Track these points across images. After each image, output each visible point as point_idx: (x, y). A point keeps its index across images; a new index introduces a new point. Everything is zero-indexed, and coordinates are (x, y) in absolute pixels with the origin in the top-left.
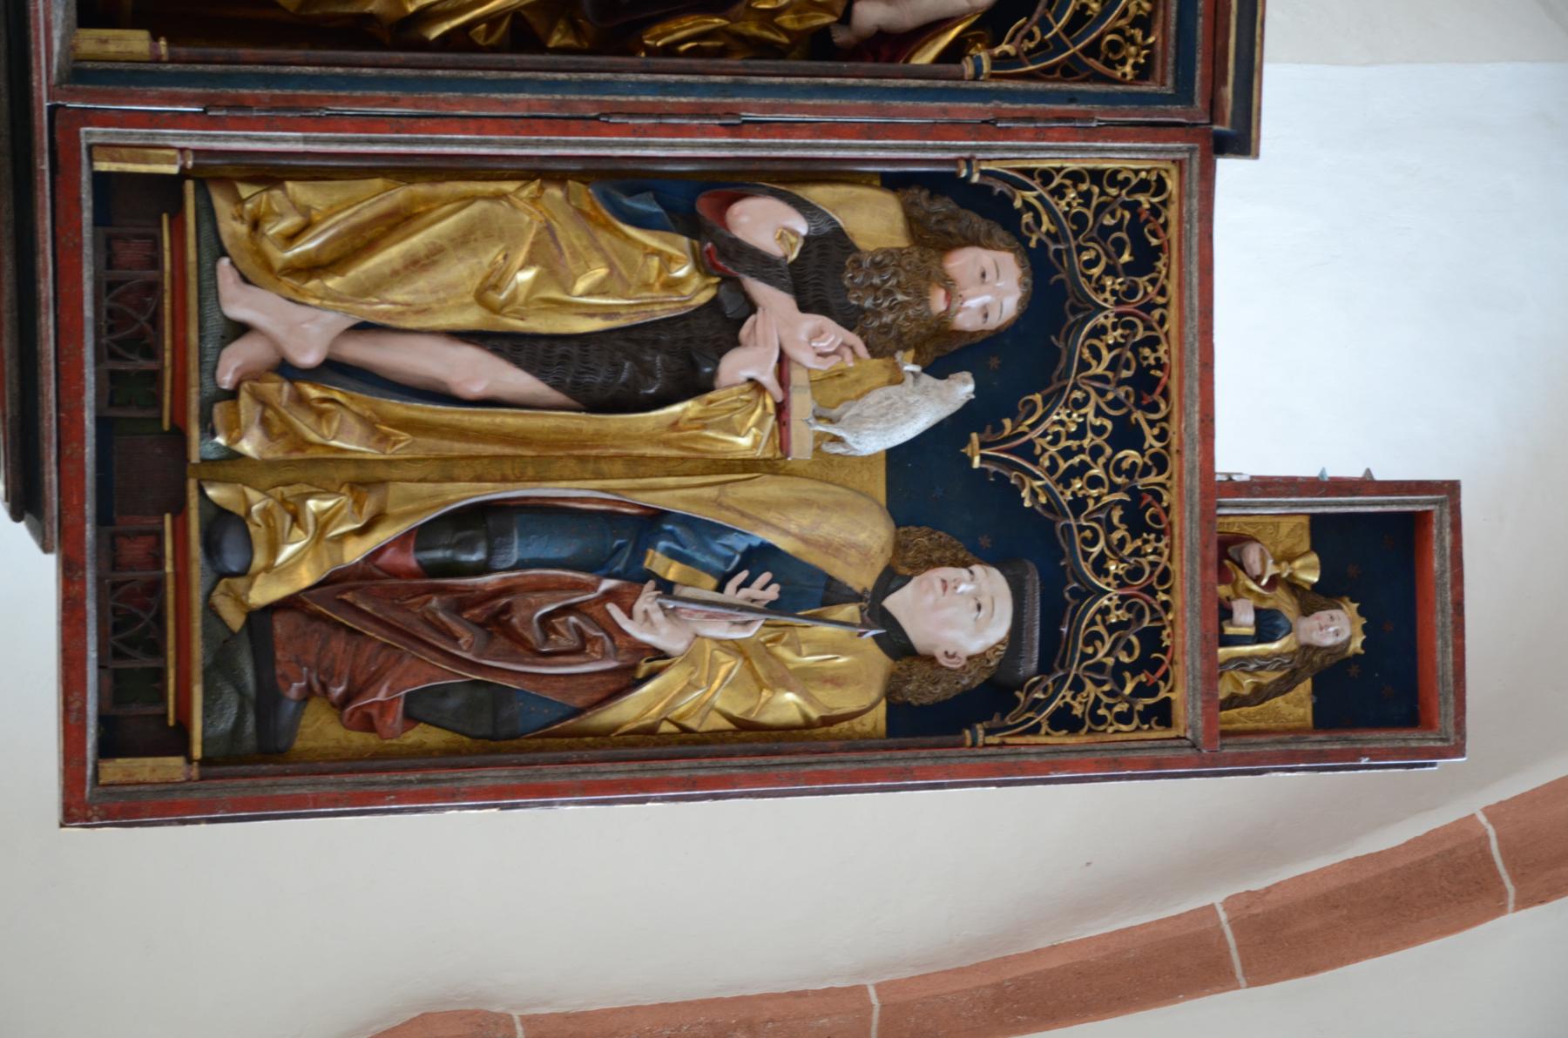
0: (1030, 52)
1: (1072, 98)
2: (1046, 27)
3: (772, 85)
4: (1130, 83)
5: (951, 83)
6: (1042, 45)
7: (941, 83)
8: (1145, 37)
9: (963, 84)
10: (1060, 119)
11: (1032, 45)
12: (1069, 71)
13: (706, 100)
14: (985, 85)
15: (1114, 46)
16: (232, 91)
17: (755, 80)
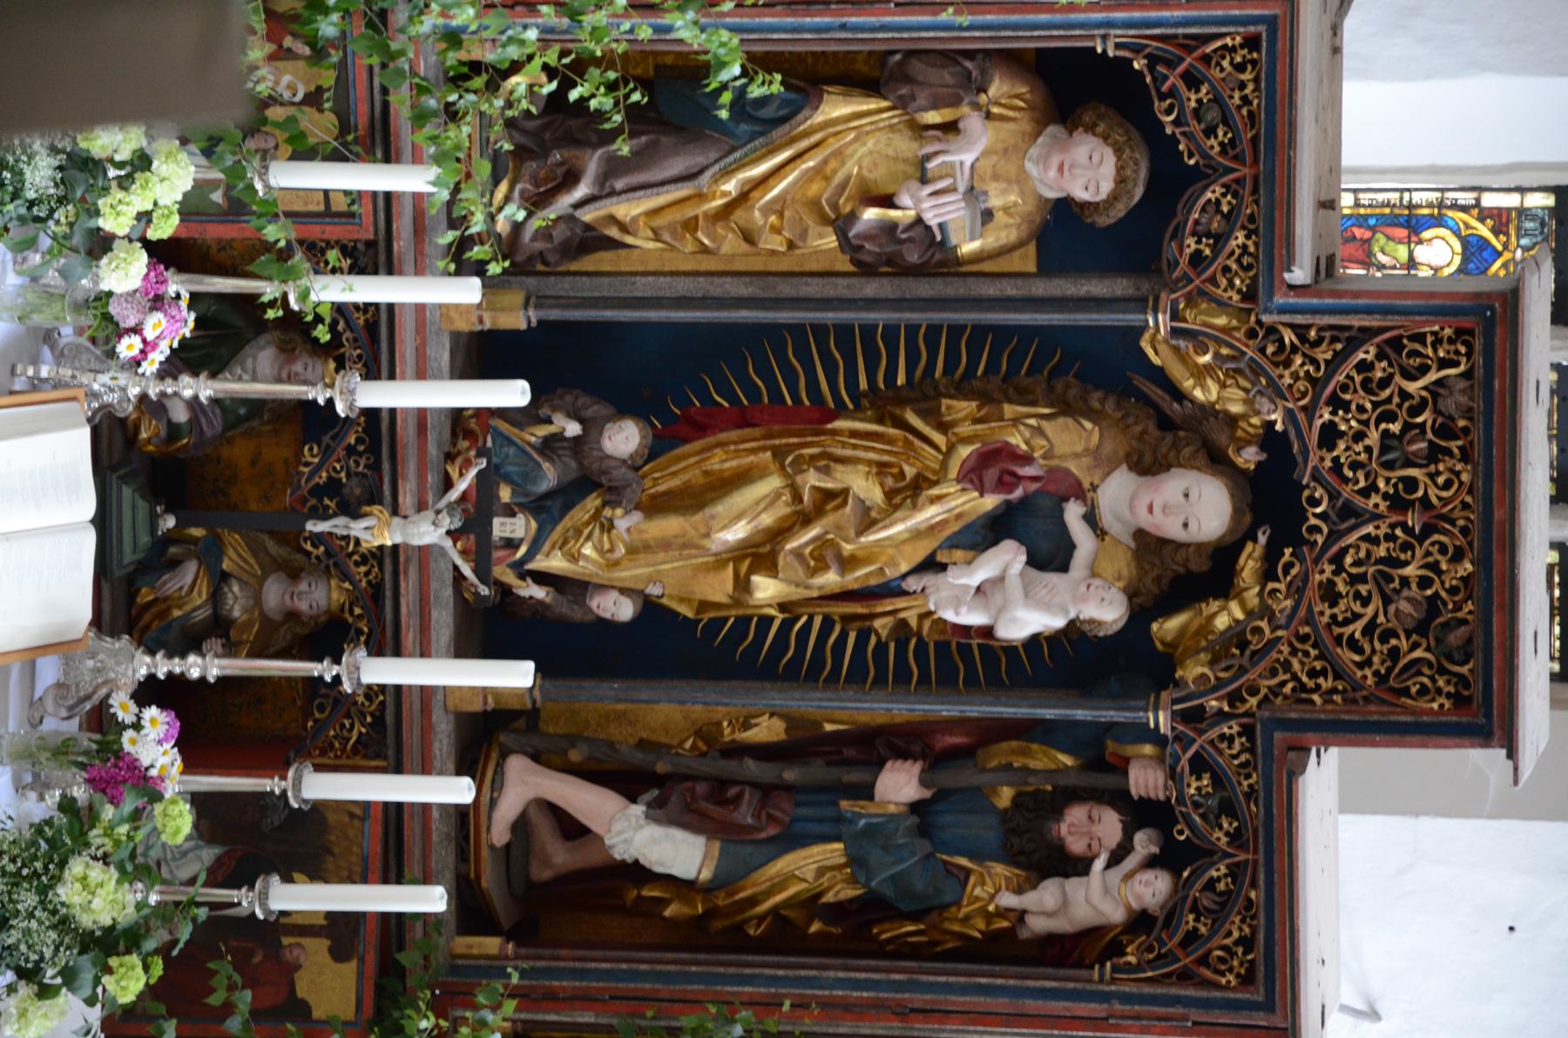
0: (1149, 962)
1: (1177, 1001)
2: (1162, 944)
3: (938, 984)
4: (1234, 989)
5: (1079, 986)
6: (1159, 957)
7: (1071, 985)
8: (1244, 954)
9: (1089, 987)
10: (1160, 1019)
11: (1151, 956)
12: (1184, 977)
13: (881, 995)
14: (1107, 988)
15: (1221, 960)
16: (547, 983)
17: (924, 978)
